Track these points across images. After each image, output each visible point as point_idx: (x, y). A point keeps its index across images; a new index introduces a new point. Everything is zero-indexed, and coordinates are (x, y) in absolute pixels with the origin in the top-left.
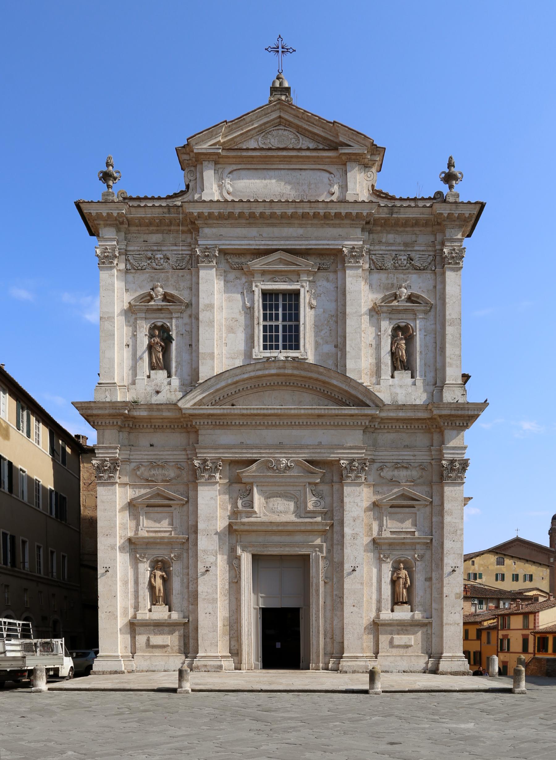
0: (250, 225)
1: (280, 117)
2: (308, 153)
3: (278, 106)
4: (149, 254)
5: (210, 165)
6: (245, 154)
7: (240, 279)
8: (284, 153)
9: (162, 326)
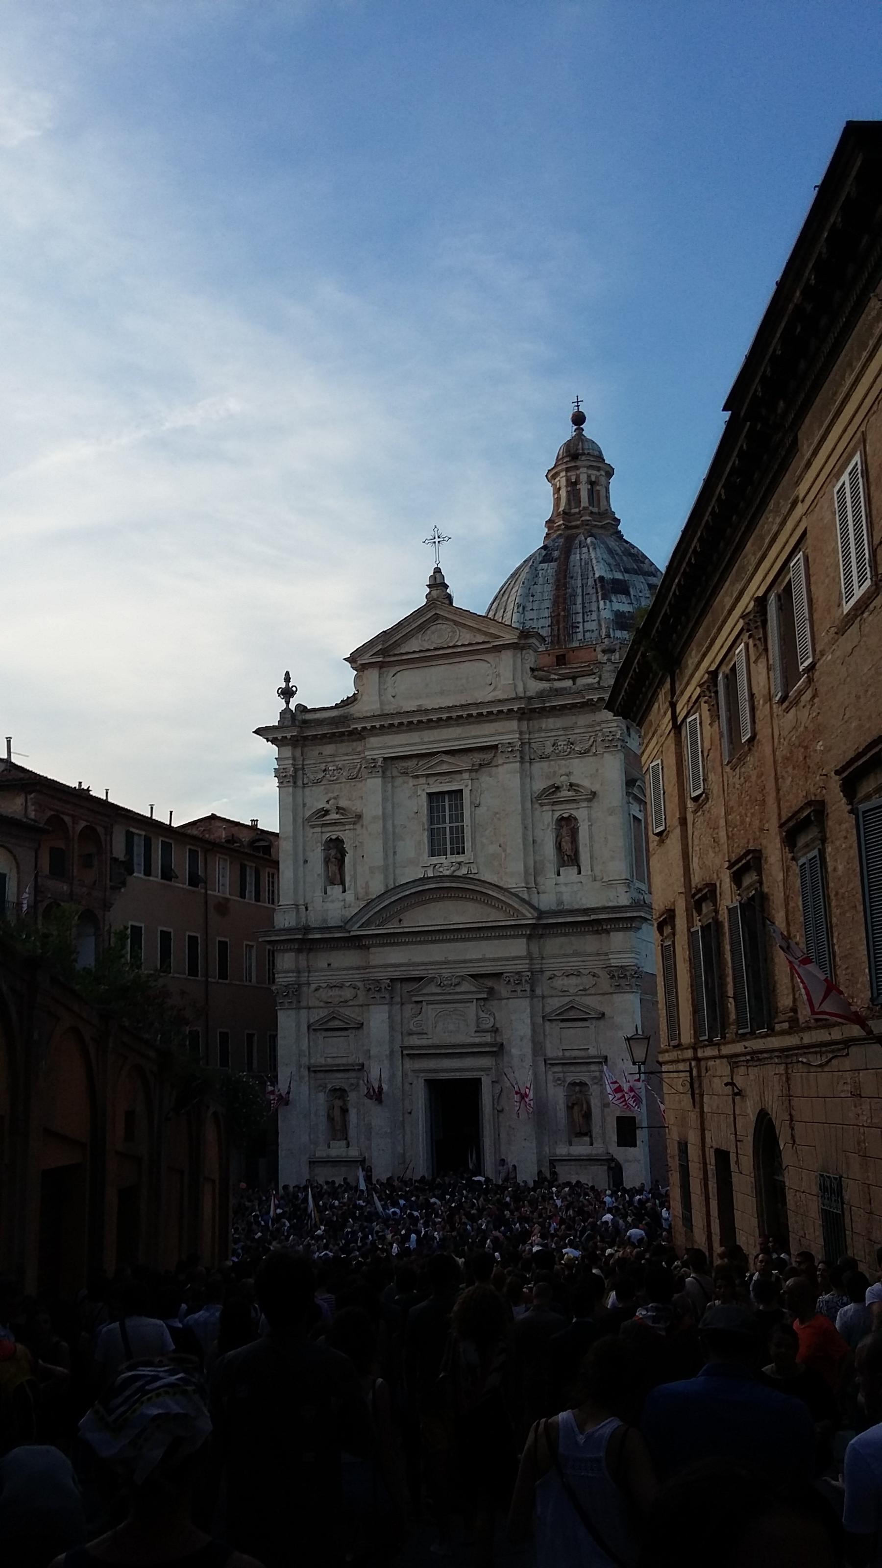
0: (410, 730)
1: (436, 614)
2: (463, 649)
3: (432, 606)
4: (323, 767)
5: (375, 671)
6: (404, 657)
7: (407, 783)
8: (441, 652)
9: (337, 838)
